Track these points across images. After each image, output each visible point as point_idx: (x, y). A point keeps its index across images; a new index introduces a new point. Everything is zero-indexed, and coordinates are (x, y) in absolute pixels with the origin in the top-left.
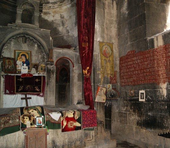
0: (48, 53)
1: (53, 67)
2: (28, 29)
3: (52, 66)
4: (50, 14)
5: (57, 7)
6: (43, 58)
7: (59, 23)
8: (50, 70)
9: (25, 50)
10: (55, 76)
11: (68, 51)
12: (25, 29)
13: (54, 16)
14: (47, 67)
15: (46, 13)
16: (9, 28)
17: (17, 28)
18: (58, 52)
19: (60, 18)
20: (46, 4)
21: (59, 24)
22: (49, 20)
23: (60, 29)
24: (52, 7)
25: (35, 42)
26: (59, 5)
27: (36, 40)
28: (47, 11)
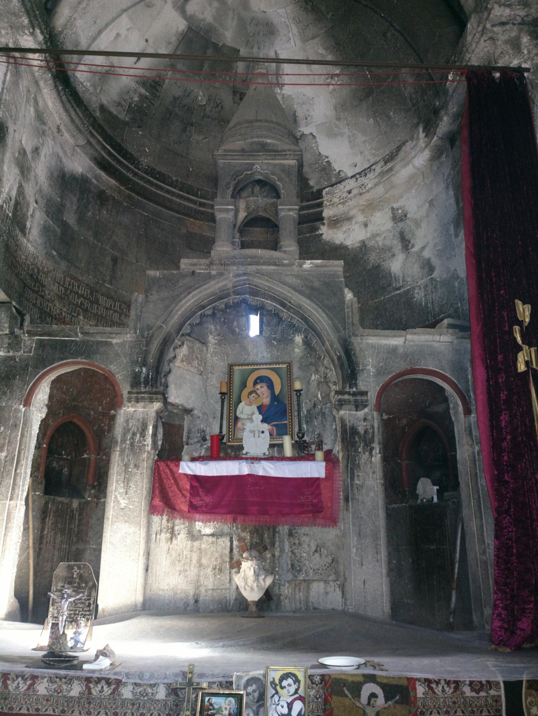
0: (339, 358)
1: (365, 418)
2: (254, 268)
3: (361, 414)
4: (349, 219)
5: (376, 185)
6: (325, 381)
7: (388, 243)
8: (354, 431)
9: (259, 361)
10: (377, 458)
11: (429, 337)
12: (242, 269)
13: (366, 225)
14: (342, 420)
15: (335, 222)
16: (185, 276)
17: (214, 272)
18: (382, 349)
19: (390, 224)
20: (332, 186)
21: (390, 249)
22: (348, 243)
23: (396, 265)
24: (354, 192)
25: (297, 330)
26: (382, 174)
27: (289, 309)
28: (340, 209)
